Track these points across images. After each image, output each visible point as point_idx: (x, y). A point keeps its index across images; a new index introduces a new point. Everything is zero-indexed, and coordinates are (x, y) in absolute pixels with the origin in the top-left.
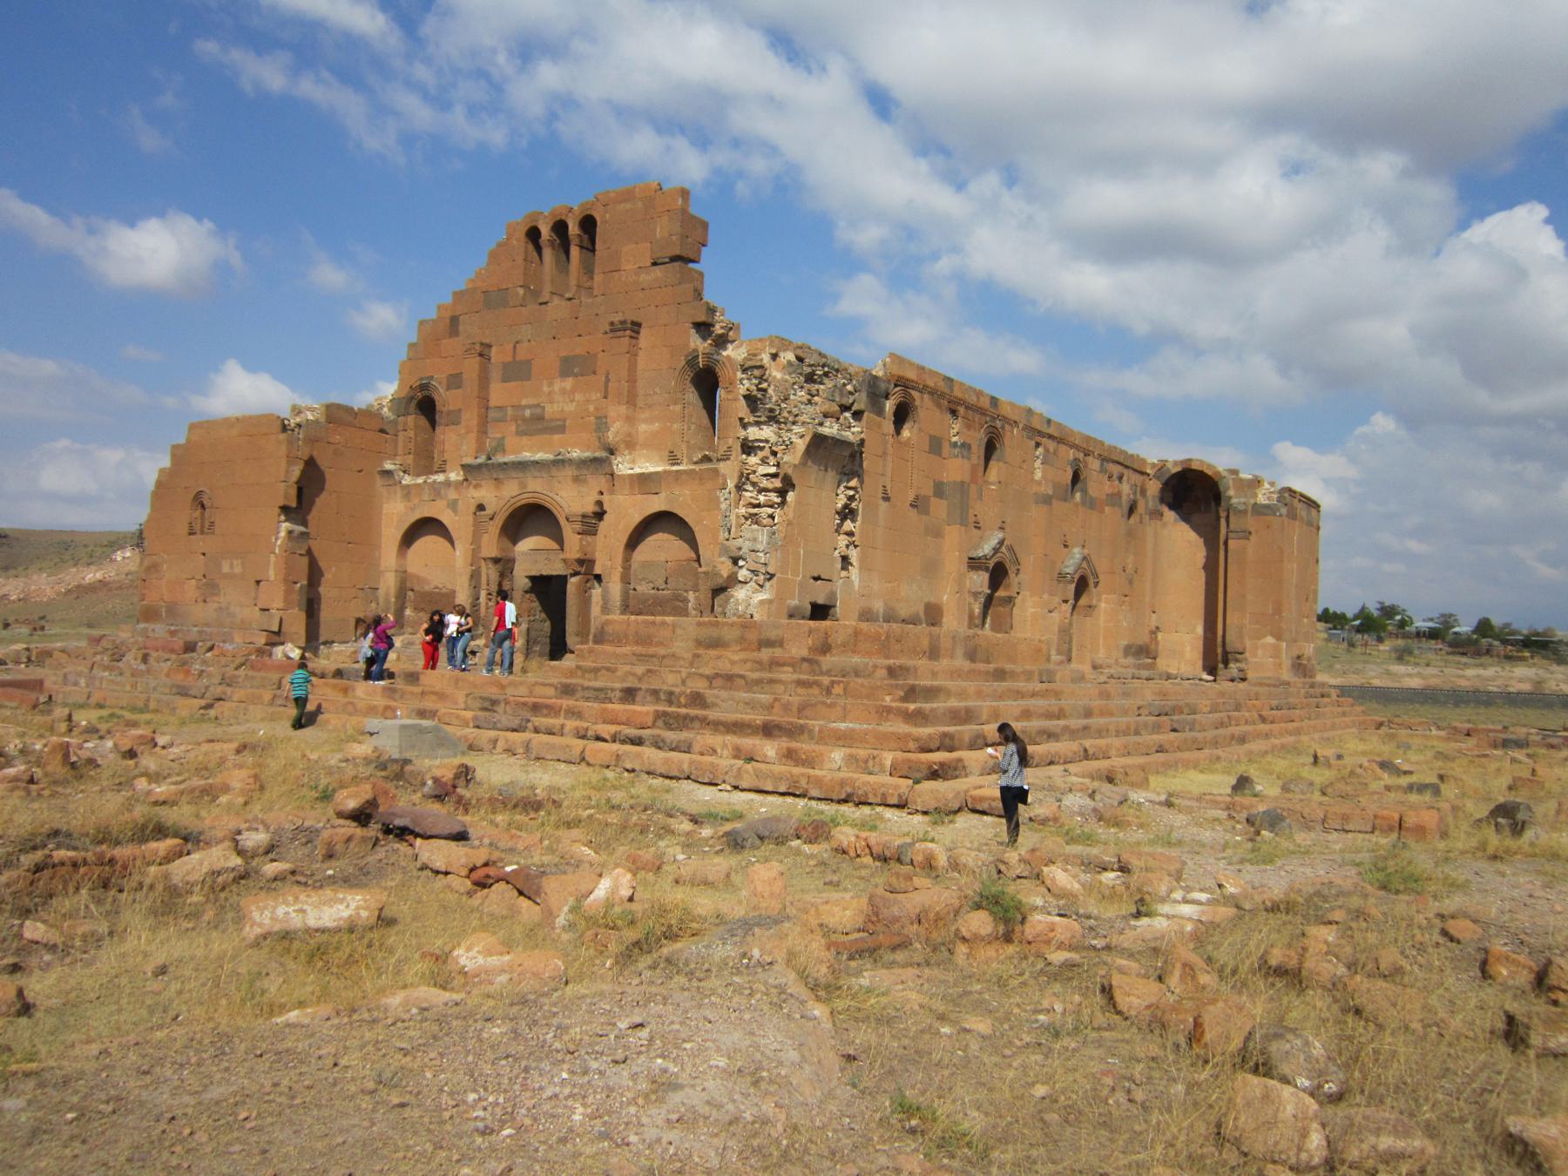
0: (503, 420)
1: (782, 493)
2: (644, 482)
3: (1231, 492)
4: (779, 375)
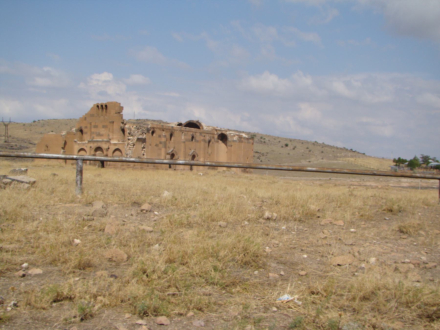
0: (94, 134)
1: (134, 146)
2: (115, 144)
3: (229, 138)
4: (133, 129)
